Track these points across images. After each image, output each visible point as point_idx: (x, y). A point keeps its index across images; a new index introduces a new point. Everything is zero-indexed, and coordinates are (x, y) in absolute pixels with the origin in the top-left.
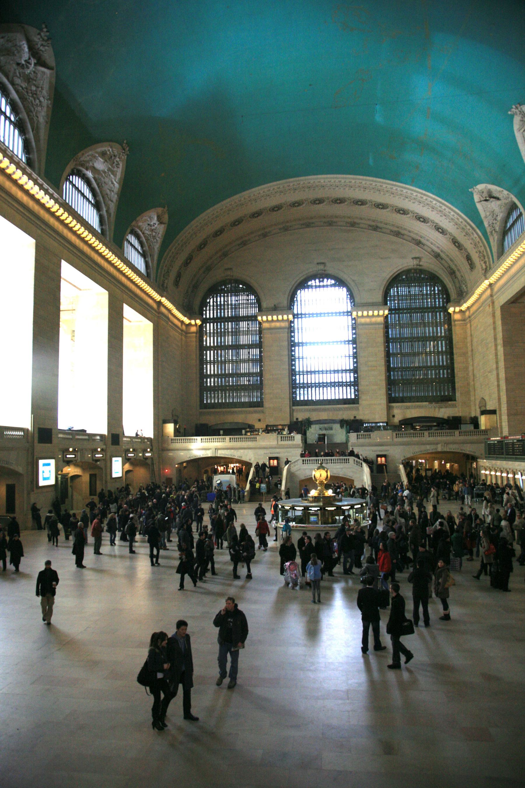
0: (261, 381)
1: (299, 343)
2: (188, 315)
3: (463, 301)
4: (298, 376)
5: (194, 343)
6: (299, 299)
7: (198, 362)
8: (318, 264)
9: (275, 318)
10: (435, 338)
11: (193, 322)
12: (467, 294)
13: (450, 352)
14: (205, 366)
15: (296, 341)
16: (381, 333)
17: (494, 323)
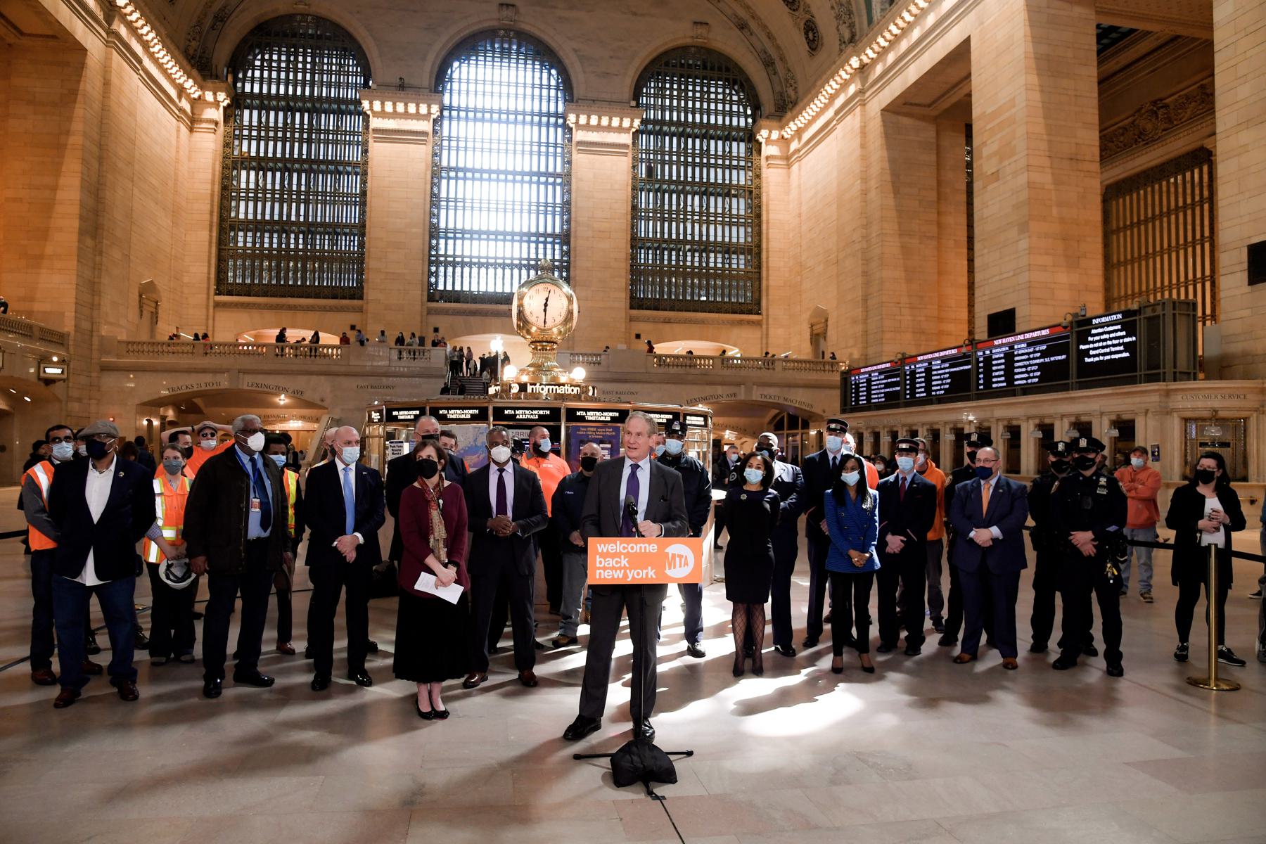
0: (361, 245)
1: (449, 169)
2: (195, 72)
3: (789, 115)
4: (442, 242)
5: (212, 146)
6: (456, 75)
7: (217, 188)
8: (502, 5)
9: (400, 107)
10: (726, 191)
11: (209, 96)
12: (795, 103)
13: (755, 218)
14: (233, 204)
15: (444, 163)
16: (624, 163)
17: (863, 146)
